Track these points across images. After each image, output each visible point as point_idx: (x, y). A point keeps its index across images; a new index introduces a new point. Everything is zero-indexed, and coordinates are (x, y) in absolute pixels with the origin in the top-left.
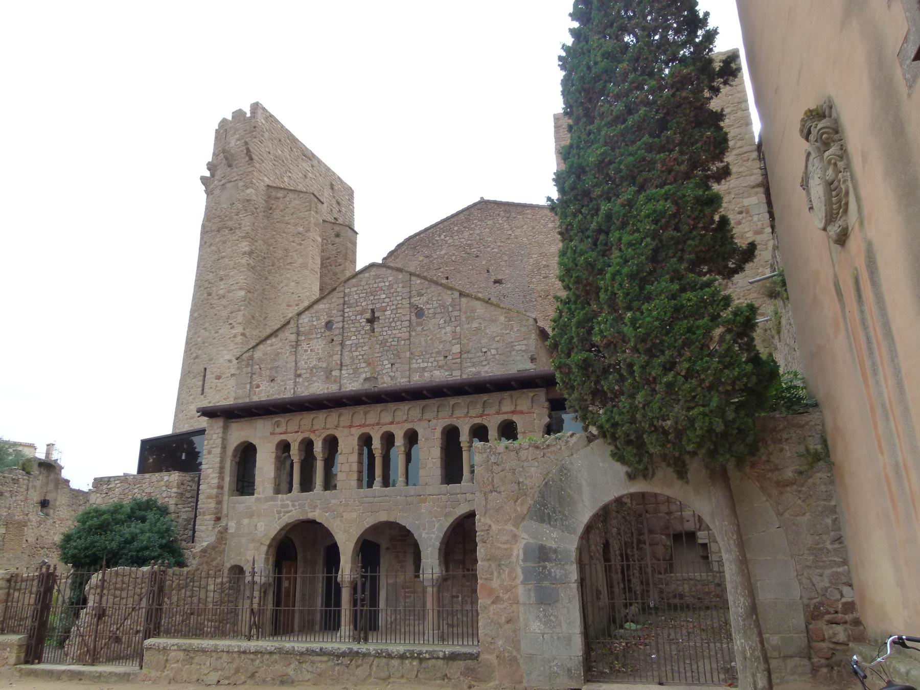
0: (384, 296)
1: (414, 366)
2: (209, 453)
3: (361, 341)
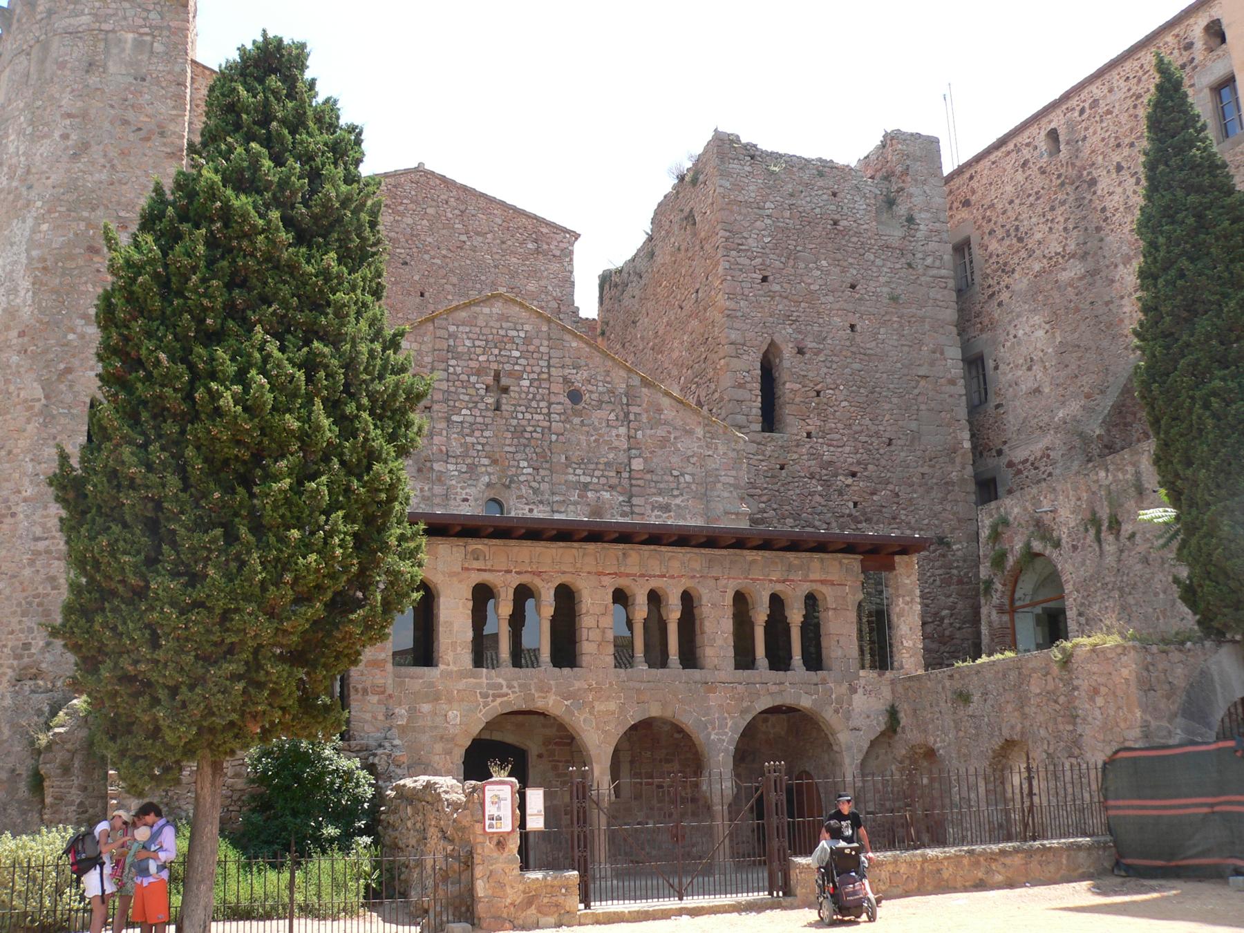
0: (517, 354)
1: (571, 477)
3: (479, 420)
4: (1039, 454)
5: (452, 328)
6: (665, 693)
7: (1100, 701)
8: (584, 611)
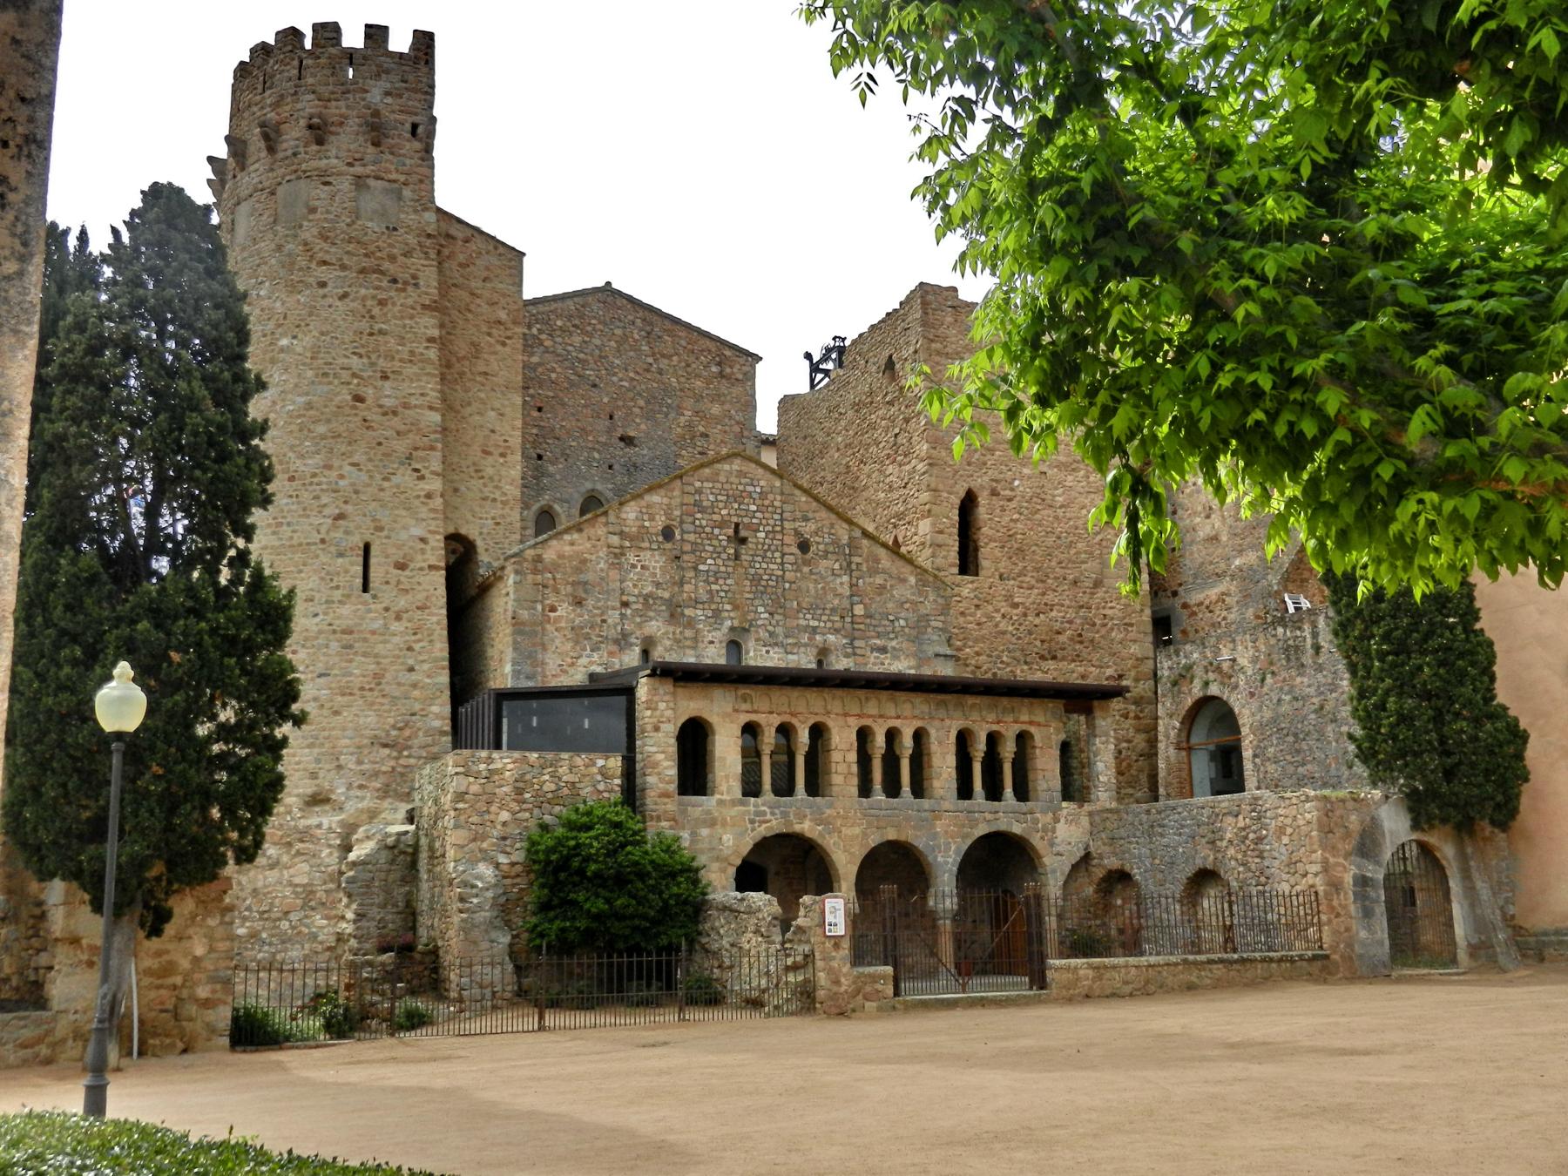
0: (754, 508)
2: (657, 729)
3: (723, 569)
4: (1214, 598)
5: (698, 484)
6: (897, 820)
7: (1285, 840)
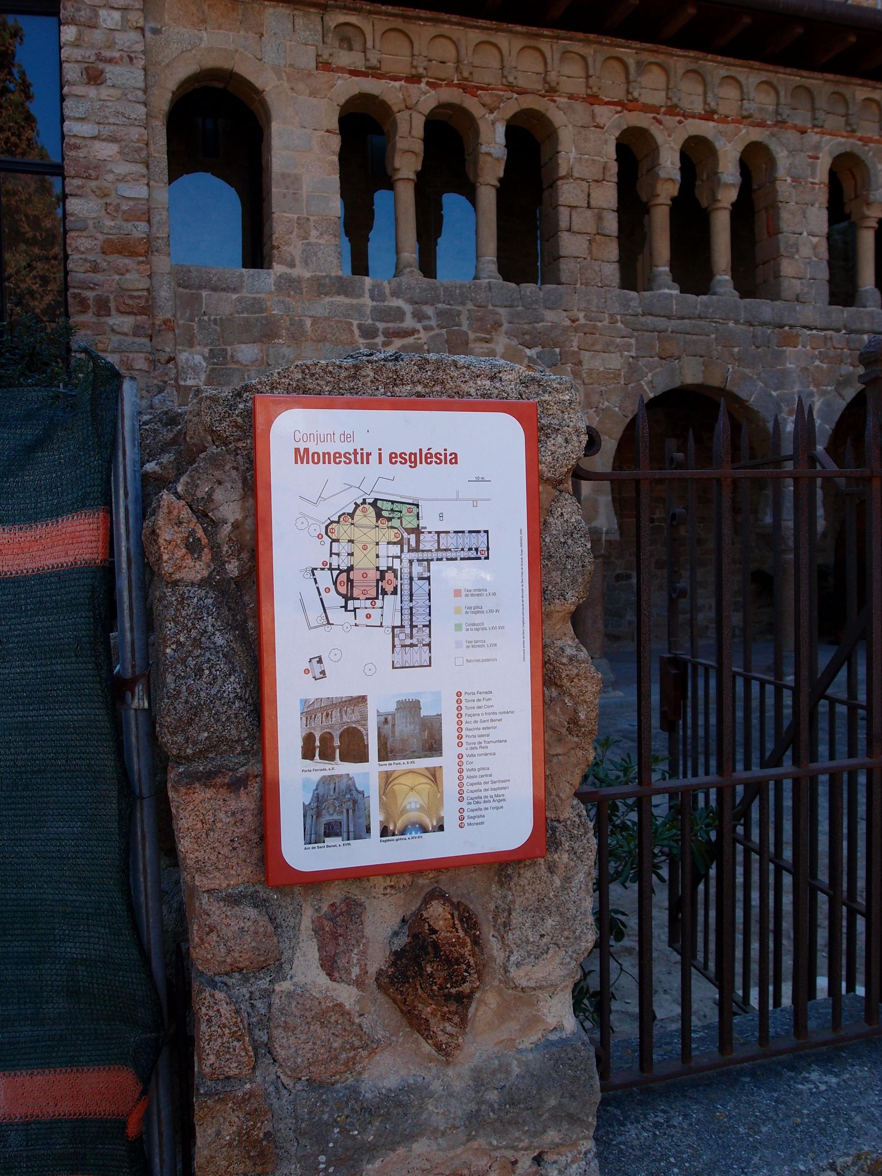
2: (94, 77)
8: (563, 171)
